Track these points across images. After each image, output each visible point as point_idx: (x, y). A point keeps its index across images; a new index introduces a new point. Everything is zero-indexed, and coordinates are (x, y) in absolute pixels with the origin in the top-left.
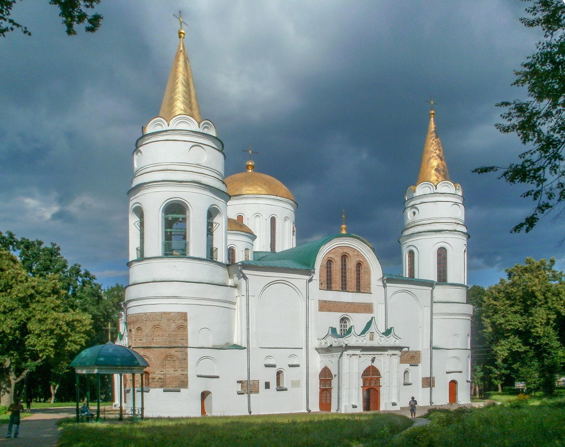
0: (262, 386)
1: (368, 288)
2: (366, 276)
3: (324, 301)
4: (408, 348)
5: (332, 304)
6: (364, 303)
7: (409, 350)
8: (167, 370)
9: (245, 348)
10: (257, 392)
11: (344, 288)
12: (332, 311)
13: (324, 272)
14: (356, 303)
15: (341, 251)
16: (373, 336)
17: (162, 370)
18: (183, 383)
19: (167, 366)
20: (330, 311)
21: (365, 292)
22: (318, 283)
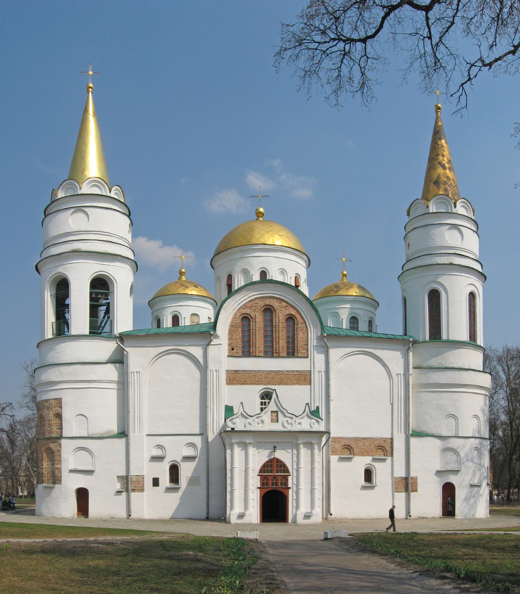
5: (246, 375)
14: (283, 372)
16: (277, 416)
20: (243, 384)
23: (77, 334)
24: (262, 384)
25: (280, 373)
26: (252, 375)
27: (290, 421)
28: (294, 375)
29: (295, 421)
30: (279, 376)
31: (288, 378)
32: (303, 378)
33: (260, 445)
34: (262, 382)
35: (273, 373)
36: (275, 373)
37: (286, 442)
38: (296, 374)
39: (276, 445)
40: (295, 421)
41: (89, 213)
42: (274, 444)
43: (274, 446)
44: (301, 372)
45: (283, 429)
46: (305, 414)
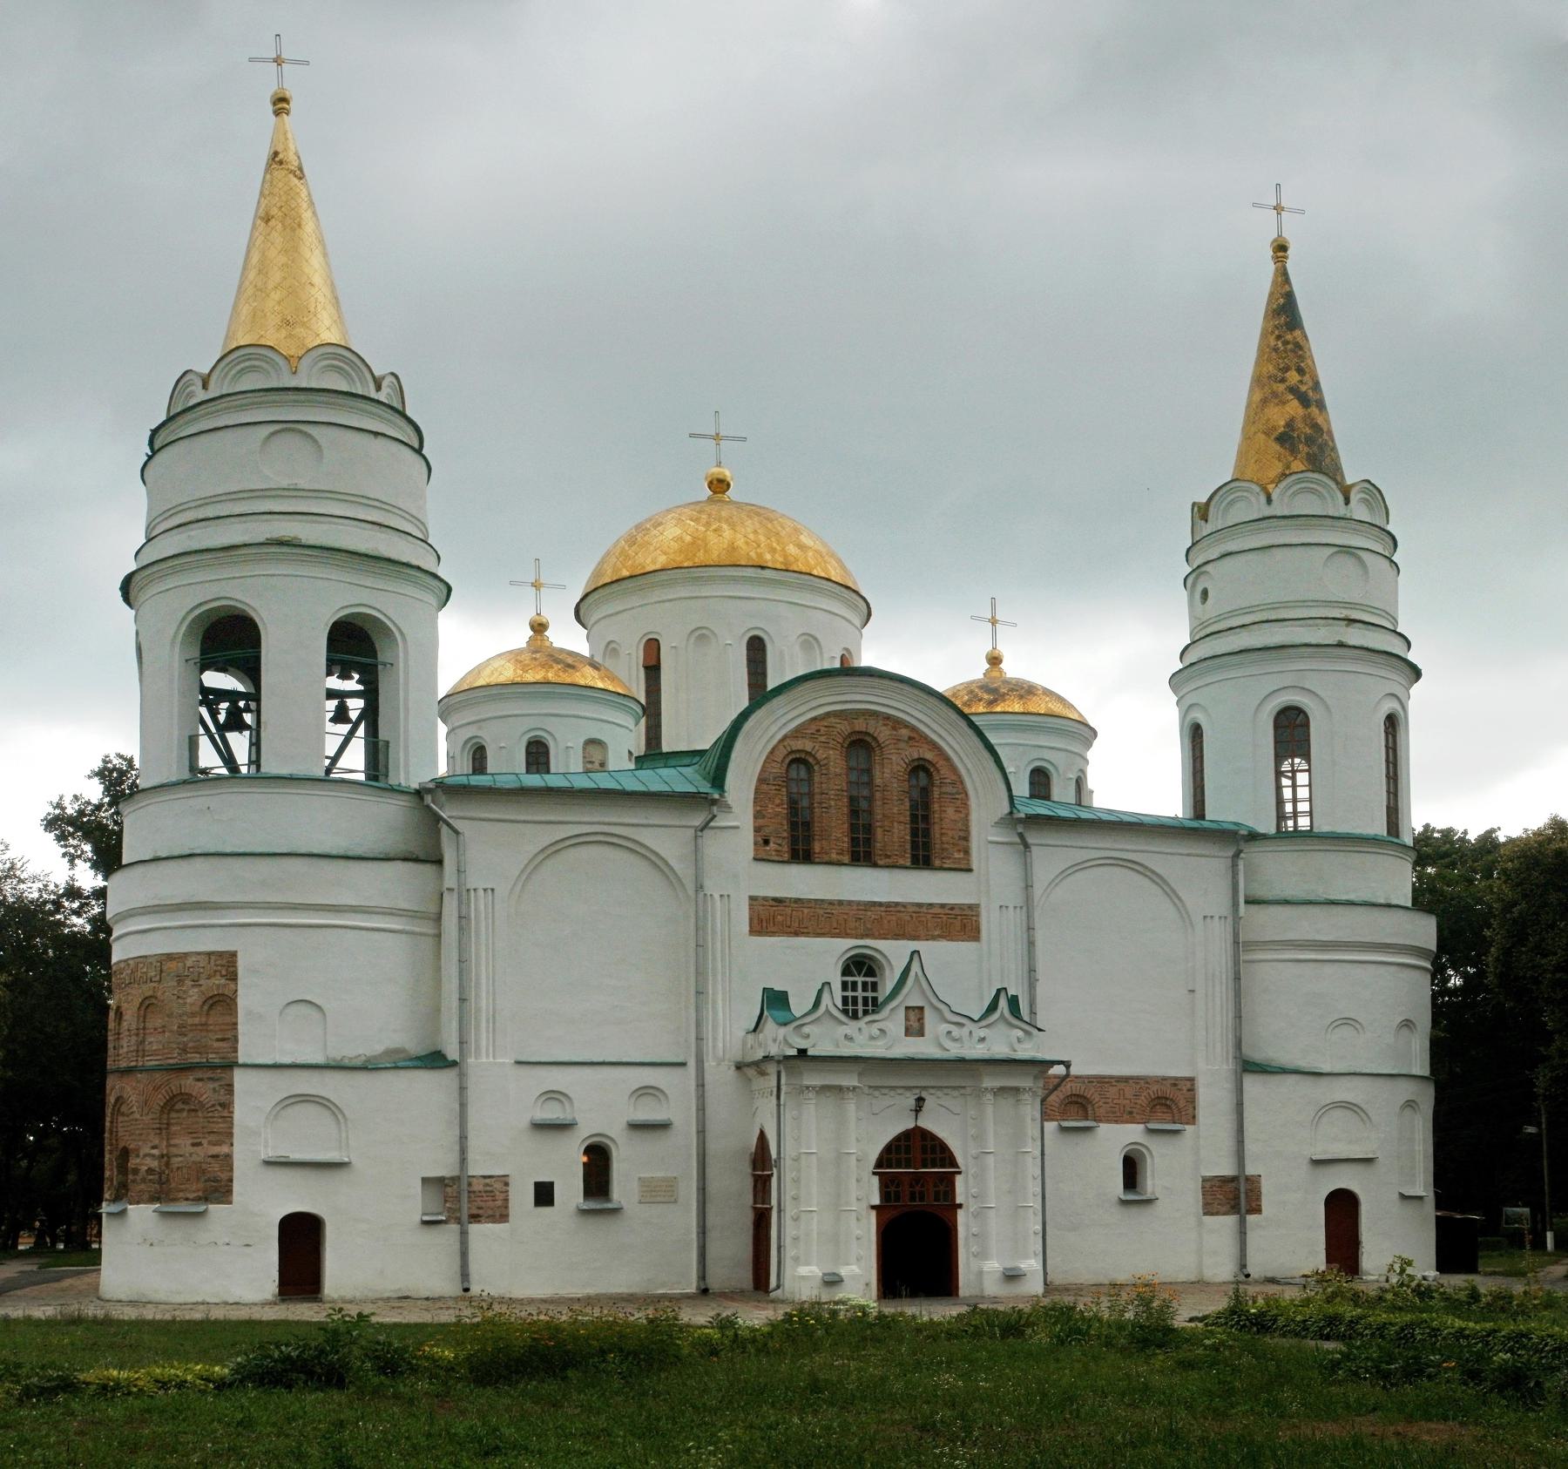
0: (521, 1196)
1: (959, 851)
2: (950, 812)
3: (775, 899)
4: (1067, 1065)
5: (806, 911)
6: (943, 906)
7: (1068, 1075)
8: (172, 1142)
9: (454, 1064)
10: (502, 1216)
11: (862, 853)
12: (807, 934)
13: (777, 801)
14: (904, 905)
15: (844, 727)
17: (156, 1142)
18: (220, 1190)
19: (174, 1128)
20: (796, 934)
21: (945, 866)
22: (747, 837)
23: (290, 772)
24: (847, 935)
25: (899, 909)
26: (821, 912)
27: (956, 1031)
28: (935, 915)
29: (971, 1032)
30: (894, 918)
31: (919, 922)
32: (958, 923)
33: (876, 1093)
34: (849, 931)
35: (878, 908)
36: (883, 909)
37: (946, 1087)
38: (939, 911)
39: (924, 1094)
40: (971, 1032)
41: (322, 441)
42: (917, 1091)
43: (916, 1097)
44: (952, 909)
45: (936, 1053)
46: (996, 1015)
